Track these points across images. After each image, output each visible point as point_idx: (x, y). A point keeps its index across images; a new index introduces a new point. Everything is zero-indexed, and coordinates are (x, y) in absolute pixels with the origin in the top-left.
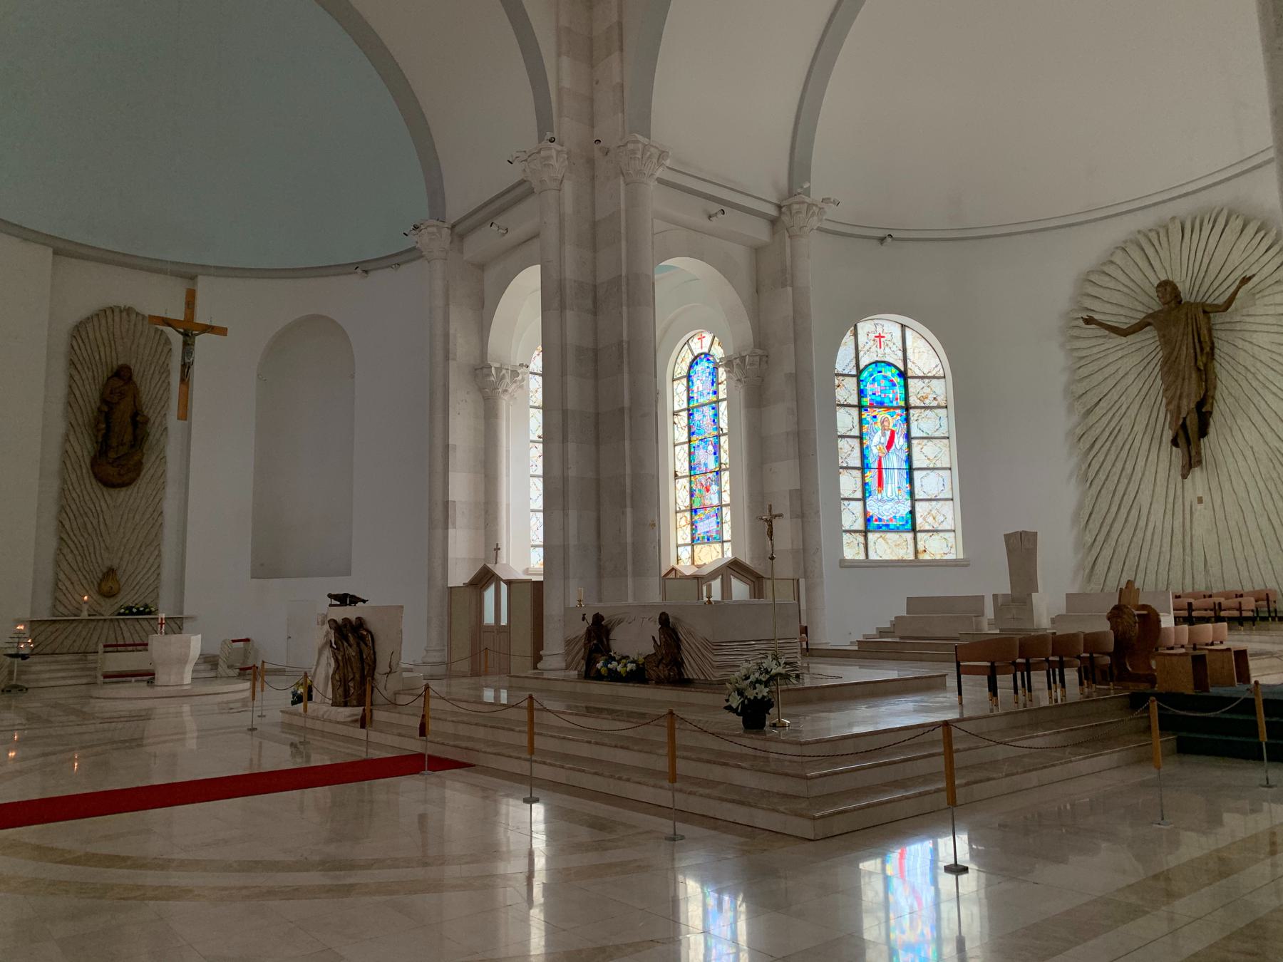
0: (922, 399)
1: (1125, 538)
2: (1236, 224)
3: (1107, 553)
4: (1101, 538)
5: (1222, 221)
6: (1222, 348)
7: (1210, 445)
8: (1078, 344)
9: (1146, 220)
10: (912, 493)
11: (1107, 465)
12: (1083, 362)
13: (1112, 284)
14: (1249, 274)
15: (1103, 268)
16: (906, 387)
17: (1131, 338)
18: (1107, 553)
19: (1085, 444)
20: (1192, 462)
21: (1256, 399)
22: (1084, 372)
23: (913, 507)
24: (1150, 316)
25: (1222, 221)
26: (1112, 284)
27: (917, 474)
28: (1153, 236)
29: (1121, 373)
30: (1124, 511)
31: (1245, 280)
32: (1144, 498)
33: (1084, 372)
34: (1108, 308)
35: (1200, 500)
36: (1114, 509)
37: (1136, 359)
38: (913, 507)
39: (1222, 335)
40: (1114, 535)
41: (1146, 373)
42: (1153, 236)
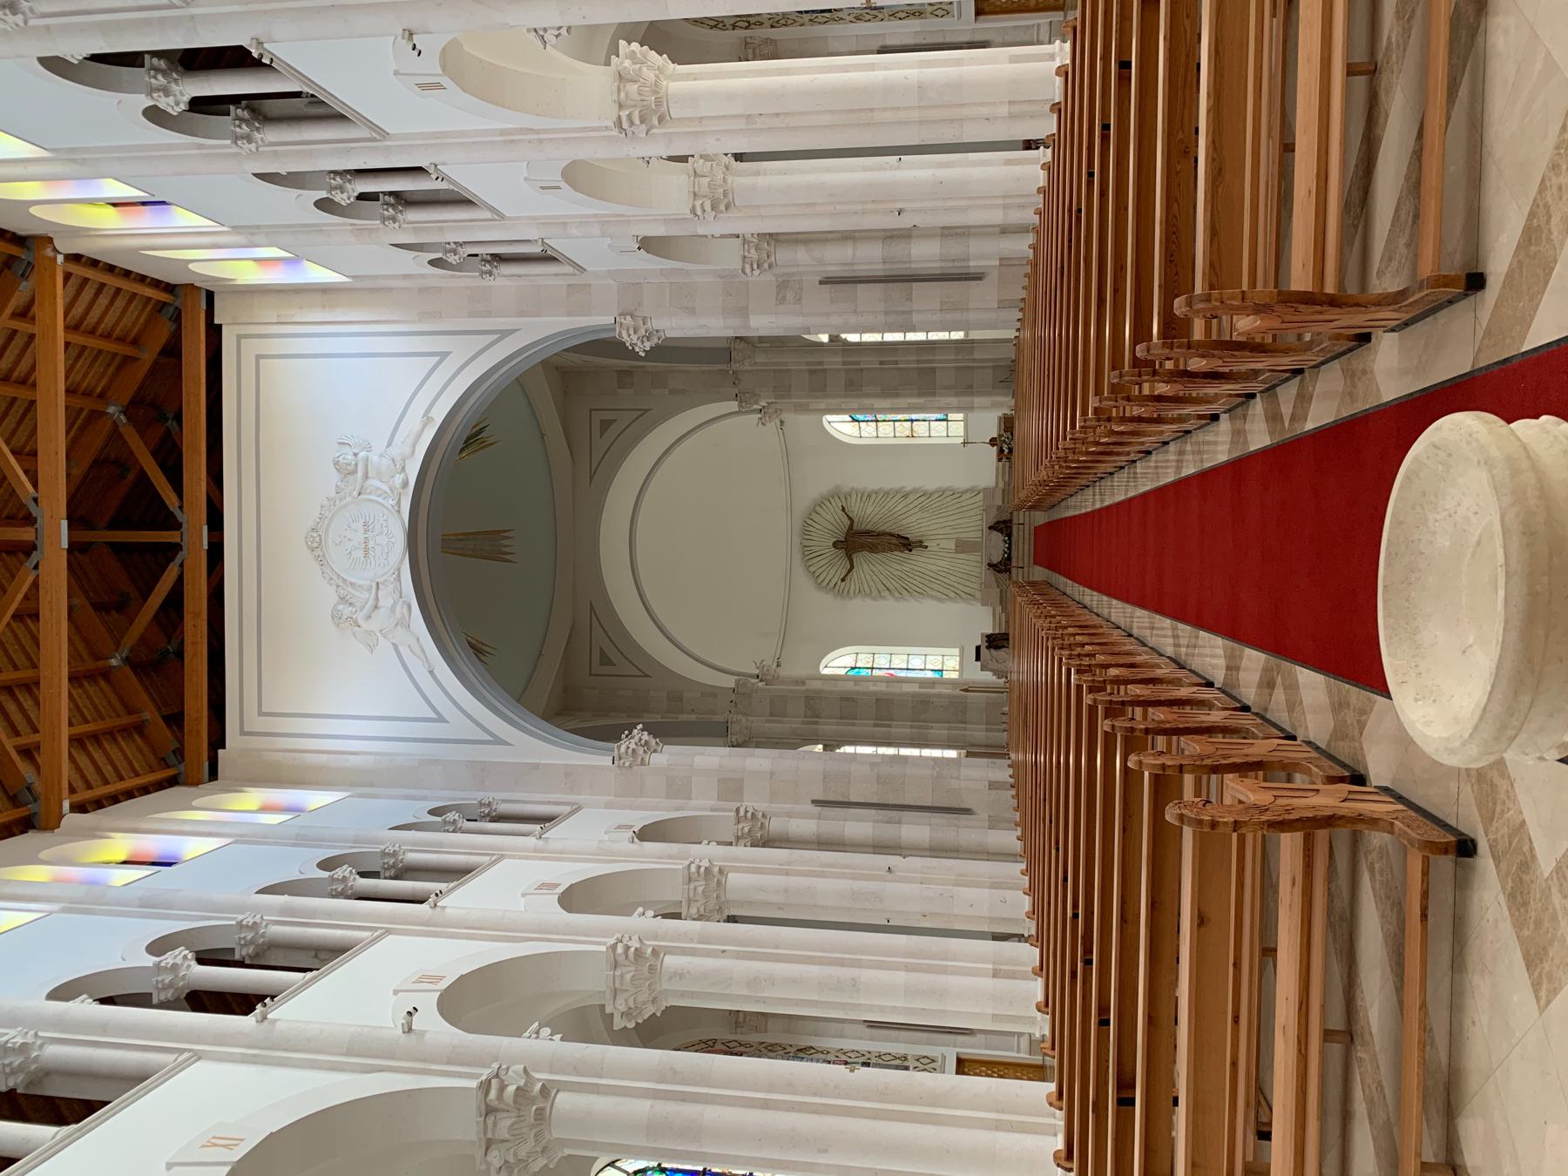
0: (868, 662)
1: (953, 578)
2: (814, 516)
3: (961, 587)
4: (952, 588)
5: (809, 522)
8: (852, 591)
9: (797, 557)
11: (915, 582)
12: (862, 589)
13: (825, 573)
15: (815, 576)
16: (860, 668)
17: (855, 564)
18: (961, 587)
19: (905, 593)
20: (920, 544)
21: (896, 515)
22: (867, 589)
24: (847, 554)
25: (809, 522)
26: (825, 573)
27: (910, 667)
28: (806, 553)
29: (872, 573)
30: (940, 578)
31: (843, 509)
32: (934, 568)
33: (867, 589)
34: (839, 572)
35: (938, 545)
36: (939, 582)
37: (865, 566)
39: (863, 527)
40: (952, 583)
41: (873, 562)
42: (806, 553)
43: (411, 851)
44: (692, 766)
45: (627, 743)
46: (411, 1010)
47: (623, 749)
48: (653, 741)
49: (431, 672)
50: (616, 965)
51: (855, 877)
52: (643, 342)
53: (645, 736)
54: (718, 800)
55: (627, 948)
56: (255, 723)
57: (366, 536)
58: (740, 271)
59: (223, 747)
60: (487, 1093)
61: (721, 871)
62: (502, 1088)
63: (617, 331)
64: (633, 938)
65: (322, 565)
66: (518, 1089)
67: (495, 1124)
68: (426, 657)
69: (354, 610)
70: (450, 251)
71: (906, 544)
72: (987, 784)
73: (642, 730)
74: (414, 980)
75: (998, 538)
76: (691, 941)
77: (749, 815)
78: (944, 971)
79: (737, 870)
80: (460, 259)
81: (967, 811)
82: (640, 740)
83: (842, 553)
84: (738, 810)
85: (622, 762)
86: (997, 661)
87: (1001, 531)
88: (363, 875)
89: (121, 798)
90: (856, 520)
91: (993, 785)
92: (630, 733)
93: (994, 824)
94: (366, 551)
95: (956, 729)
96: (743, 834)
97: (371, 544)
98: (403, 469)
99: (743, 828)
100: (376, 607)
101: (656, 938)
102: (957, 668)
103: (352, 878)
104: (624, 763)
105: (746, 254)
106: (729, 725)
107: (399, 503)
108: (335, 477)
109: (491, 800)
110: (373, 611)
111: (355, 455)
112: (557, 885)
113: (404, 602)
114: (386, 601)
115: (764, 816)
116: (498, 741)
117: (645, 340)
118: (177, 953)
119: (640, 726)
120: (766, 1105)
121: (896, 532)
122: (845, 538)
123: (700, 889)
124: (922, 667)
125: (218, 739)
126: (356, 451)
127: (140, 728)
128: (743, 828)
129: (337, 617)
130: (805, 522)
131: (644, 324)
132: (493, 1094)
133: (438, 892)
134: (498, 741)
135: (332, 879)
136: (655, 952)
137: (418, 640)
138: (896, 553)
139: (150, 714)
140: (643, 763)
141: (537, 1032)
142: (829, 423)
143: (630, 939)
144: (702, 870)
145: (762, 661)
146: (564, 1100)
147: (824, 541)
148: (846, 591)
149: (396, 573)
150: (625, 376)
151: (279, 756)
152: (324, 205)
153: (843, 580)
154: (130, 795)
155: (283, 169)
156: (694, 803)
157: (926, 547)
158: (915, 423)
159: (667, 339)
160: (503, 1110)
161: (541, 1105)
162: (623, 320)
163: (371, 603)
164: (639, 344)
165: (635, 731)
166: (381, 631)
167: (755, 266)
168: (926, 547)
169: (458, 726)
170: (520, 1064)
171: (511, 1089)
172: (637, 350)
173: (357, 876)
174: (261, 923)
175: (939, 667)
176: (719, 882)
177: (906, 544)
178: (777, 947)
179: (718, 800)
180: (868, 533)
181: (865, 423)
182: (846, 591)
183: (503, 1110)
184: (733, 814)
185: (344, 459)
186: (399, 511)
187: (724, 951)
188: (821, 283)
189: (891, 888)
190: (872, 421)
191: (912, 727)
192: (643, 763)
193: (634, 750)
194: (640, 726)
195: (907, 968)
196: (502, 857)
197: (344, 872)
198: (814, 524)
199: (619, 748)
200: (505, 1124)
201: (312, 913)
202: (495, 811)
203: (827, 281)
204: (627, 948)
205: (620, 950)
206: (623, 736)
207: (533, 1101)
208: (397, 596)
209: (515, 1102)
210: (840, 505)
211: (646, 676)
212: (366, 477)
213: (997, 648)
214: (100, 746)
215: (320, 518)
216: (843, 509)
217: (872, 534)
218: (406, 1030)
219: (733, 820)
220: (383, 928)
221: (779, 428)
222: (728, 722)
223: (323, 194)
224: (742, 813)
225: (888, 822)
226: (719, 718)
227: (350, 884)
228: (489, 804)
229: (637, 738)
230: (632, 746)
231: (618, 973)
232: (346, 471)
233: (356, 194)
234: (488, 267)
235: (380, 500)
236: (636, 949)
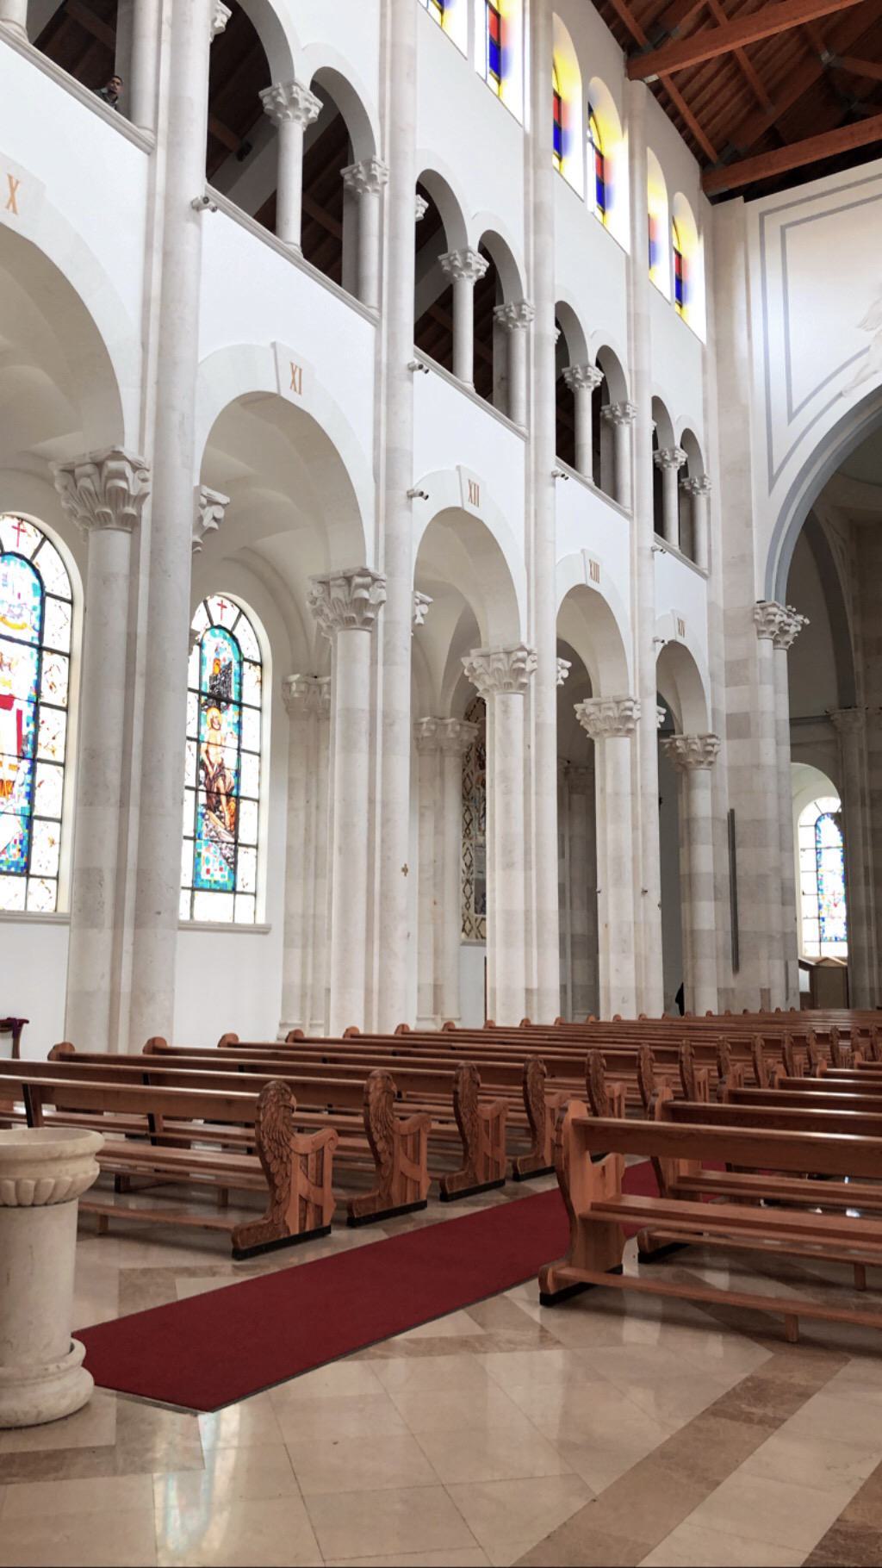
43: (631, 429)
44: (761, 683)
45: (780, 613)
46: (425, 494)
47: (774, 610)
48: (789, 638)
49: (840, 395)
50: (508, 653)
51: (634, 859)
55: (523, 661)
56: (773, 225)
59: (746, 200)
60: (360, 575)
61: (630, 731)
62: (366, 587)
64: (535, 664)
66: (366, 600)
67: (340, 586)
68: (858, 385)
72: (766, 987)
73: (803, 625)
74: (472, 480)
76: (537, 716)
77: (709, 748)
78: (527, 944)
79: (633, 745)
81: (736, 967)
82: (789, 625)
84: (712, 736)
85: (759, 611)
89: (677, 121)
91: (765, 994)
92: (795, 613)
93: (723, 993)
95: (870, 957)
96: (690, 744)
99: (696, 743)
101: (538, 684)
103: (590, 384)
104: (758, 613)
106: (853, 709)
109: (708, 487)
112: (597, 579)
115: (711, 763)
116: (772, 480)
118: (481, 262)
119: (807, 621)
120: (371, 801)
123: (610, 713)
125: (752, 192)
127: (757, 108)
128: (696, 743)
132: (358, 580)
134: (772, 480)
136: (523, 686)
137: (875, 372)
139: (773, 113)
140: (760, 632)
141: (422, 602)
143: (533, 662)
144: (629, 713)
146: (364, 637)
151: (740, 260)
154: (682, 128)
156: (723, 692)
160: (350, 590)
161: (357, 620)
165: (800, 618)
169: (784, 436)
170: (388, 596)
171: (365, 594)
174: (526, 321)
178: (537, 793)
179: (728, 715)
183: (350, 590)
184: (710, 731)
187: (529, 747)
191: (868, 908)
192: (760, 632)
193: (772, 621)
194: (807, 621)
195: (527, 912)
200: (338, 593)
201: (539, 364)
204: (523, 661)
206: (789, 607)
207: (360, 612)
209: (356, 600)
214: (730, 79)
218: (410, 494)
219: (702, 732)
220: (530, 433)
222: (856, 707)
224: (713, 741)
225: (715, 887)
226: (861, 698)
228: (703, 486)
229: (790, 621)
230: (778, 619)
236: (523, 669)
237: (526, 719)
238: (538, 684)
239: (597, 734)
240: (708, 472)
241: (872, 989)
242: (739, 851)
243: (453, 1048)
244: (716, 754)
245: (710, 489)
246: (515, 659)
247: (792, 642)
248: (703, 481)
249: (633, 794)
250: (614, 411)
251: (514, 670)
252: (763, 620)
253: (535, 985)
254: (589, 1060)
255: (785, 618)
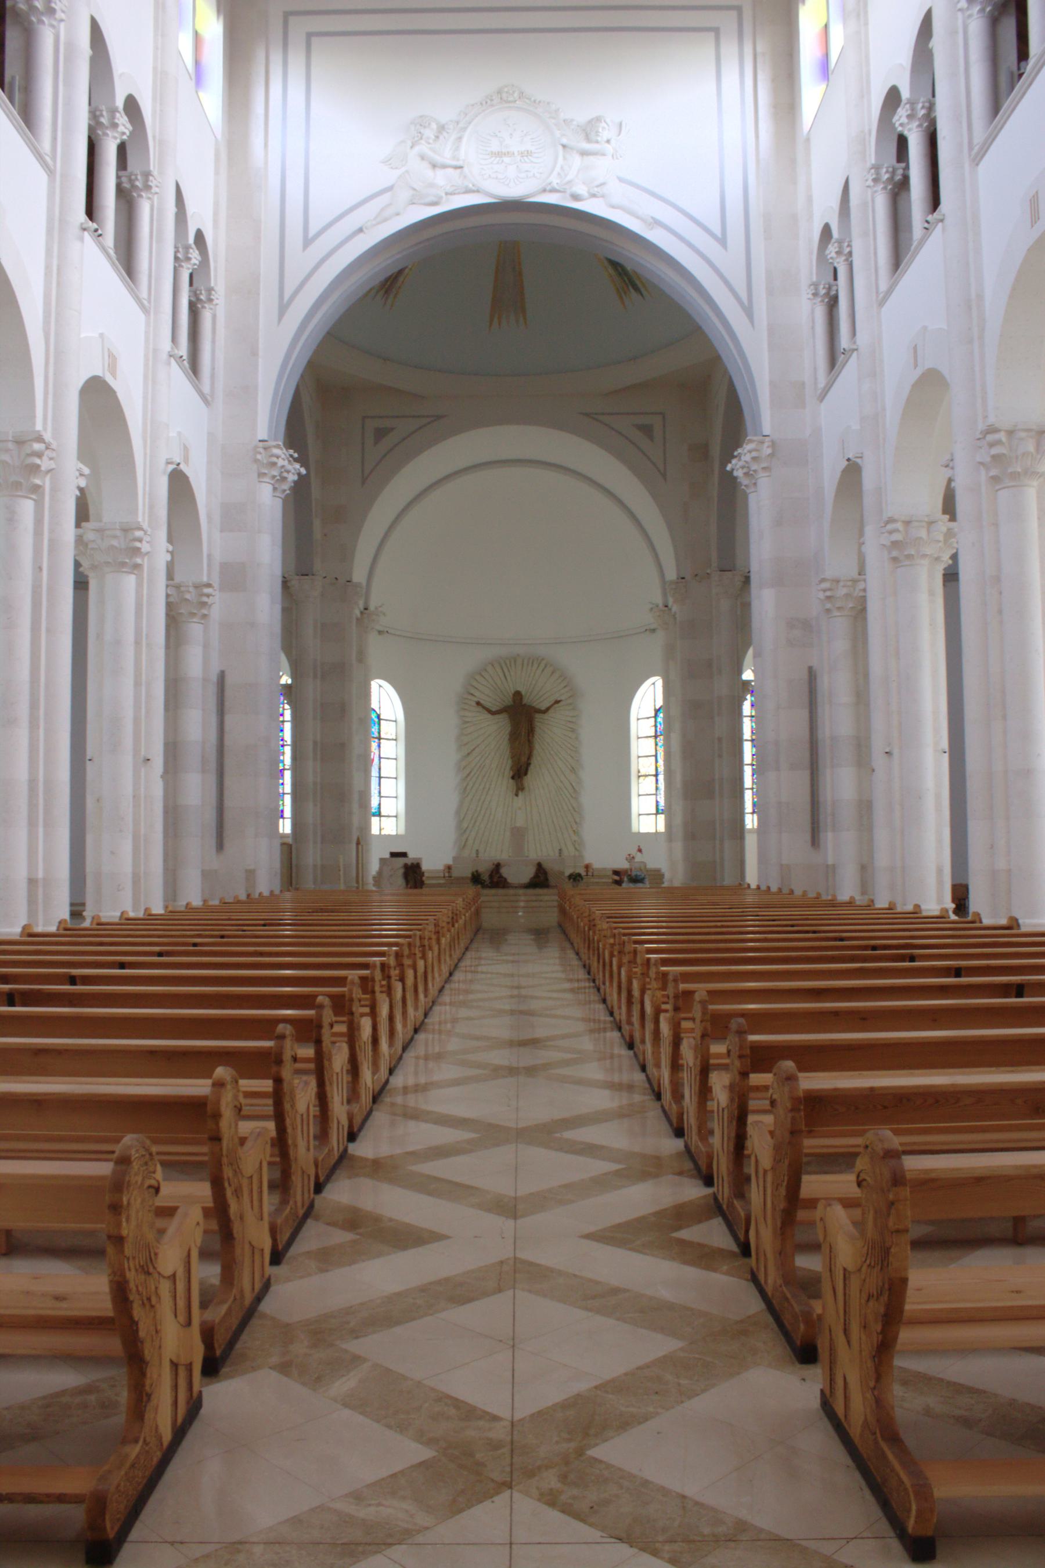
0: (386, 733)
4: (471, 826)
5: (542, 665)
6: (538, 731)
7: (529, 780)
8: (467, 714)
10: (380, 792)
14: (559, 699)
16: (379, 724)
17: (497, 716)
20: (520, 788)
23: (380, 801)
25: (542, 665)
28: (508, 663)
31: (557, 702)
35: (520, 809)
38: (380, 801)
39: (538, 724)
40: (477, 824)
47: (276, 451)
48: (286, 486)
49: (360, 230)
50: (20, 443)
51: (136, 720)
52: (743, 467)
53: (292, 477)
54: (221, 563)
55: (39, 455)
57: (516, 154)
58: (823, 577)
63: (755, 438)
64: (52, 462)
65: (481, 104)
68: (379, 223)
69: (431, 141)
70: (840, 247)
71: (520, 772)
72: (252, 867)
73: (299, 474)
75: (527, 874)
76: (52, 531)
77: (205, 599)
79: (139, 585)
80: (831, 258)
81: (220, 846)
82: (288, 472)
83: (508, 701)
84: (209, 585)
85: (261, 450)
86: (391, 876)
87: (536, 876)
88: (122, 149)
90: (545, 716)
91: (250, 875)
93: (207, 875)
94: (499, 154)
96: (182, 592)
97: (506, 160)
98: (594, 196)
99: (189, 592)
100: (434, 166)
102: (383, 833)
103: (116, 135)
104: (260, 453)
105: (841, 584)
107: (553, 190)
108: (582, 117)
110: (430, 163)
111: (608, 141)
112: (114, 374)
113: (441, 198)
114: (441, 179)
115: (205, 616)
116: (283, 308)
117: (745, 470)
121: (535, 761)
122: (525, 705)
123: (115, 543)
124: (382, 795)
126: (613, 142)
128: (189, 592)
129: (421, 122)
130: (543, 659)
131: (764, 468)
133: (100, 232)
134: (283, 308)
135: (113, 111)
137: (398, 214)
138: (510, 761)
140: (261, 475)
142: (654, 684)
143: (51, 459)
144: (138, 544)
145: (384, 614)
147: (519, 681)
148: (466, 707)
149: (474, 188)
150: (701, 452)
152: (893, 97)
153: (478, 703)
155: (938, 43)
157: (517, 795)
158: (654, 778)
159: (746, 497)
162: (766, 444)
163: (438, 159)
164: (741, 463)
165: (297, 466)
166: (407, 171)
167: (828, 593)
168: (517, 795)
169: (299, 263)
172: (734, 461)
173: (118, 141)
175: (383, 813)
176: (123, 564)
177: (520, 772)
178: (48, 630)
179: (221, 563)
180: (531, 731)
181: (653, 724)
182: (466, 707)
184: (205, 579)
185: (603, 128)
186: (544, 191)
188: (810, 669)
189: (127, 761)
190: (656, 731)
192: (261, 475)
193: (274, 464)
194: (303, 471)
195: (32, 782)
196: (145, 310)
197: (124, 125)
198: (541, 668)
199: (278, 447)
202: (205, 307)
203: (812, 676)
204: (39, 455)
205: (37, 446)
206: (291, 452)
208: (449, 189)
210: (563, 698)
211: (364, 481)
212: (584, 153)
213: (406, 876)
215: (535, 101)
216: (557, 702)
217: (531, 735)
221: (648, 628)
222: (313, 575)
223: (905, 94)
224: (207, 591)
225: (203, 757)
227: (44, 19)
228: (210, 300)
229: (289, 467)
230: (280, 462)
231: (10, 445)
232: (589, 130)
233: (906, 133)
234: (823, 292)
235: (558, 169)
236: (39, 466)
237: (38, 533)
238: (54, 490)
239: (94, 567)
240: (216, 284)
241: (315, 866)
242: (228, 719)
243: (73, 980)
244: (210, 606)
245: (217, 304)
246: (29, 452)
247: (288, 492)
248: (210, 294)
249: (138, 643)
250: (134, 181)
251: (27, 466)
252: (265, 462)
253: (40, 875)
254: (351, 991)
255: (286, 463)
